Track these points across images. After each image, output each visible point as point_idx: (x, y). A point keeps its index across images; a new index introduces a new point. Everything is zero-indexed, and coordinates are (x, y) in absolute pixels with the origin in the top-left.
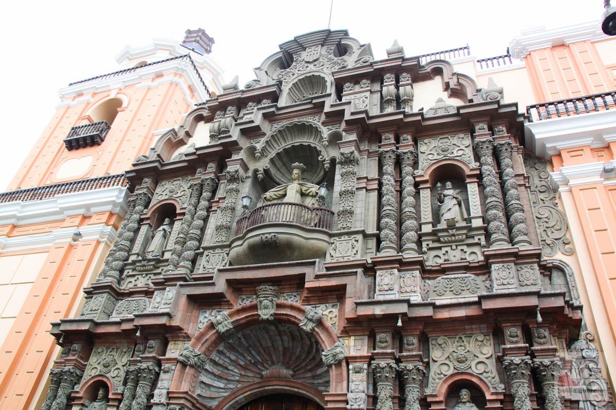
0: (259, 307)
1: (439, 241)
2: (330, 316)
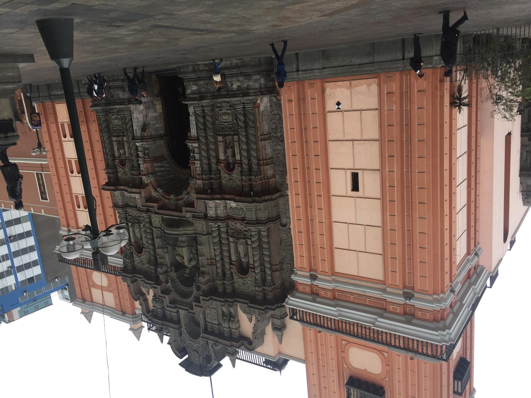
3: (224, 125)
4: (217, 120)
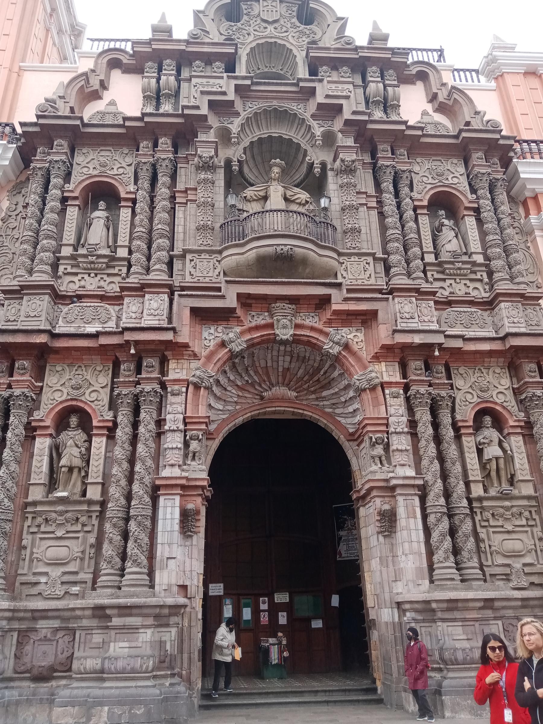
0: (275, 327)
1: (443, 272)
2: (356, 340)
3: (68, 532)
4: (92, 546)
